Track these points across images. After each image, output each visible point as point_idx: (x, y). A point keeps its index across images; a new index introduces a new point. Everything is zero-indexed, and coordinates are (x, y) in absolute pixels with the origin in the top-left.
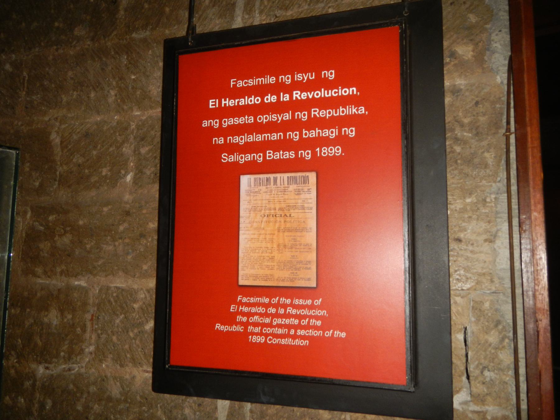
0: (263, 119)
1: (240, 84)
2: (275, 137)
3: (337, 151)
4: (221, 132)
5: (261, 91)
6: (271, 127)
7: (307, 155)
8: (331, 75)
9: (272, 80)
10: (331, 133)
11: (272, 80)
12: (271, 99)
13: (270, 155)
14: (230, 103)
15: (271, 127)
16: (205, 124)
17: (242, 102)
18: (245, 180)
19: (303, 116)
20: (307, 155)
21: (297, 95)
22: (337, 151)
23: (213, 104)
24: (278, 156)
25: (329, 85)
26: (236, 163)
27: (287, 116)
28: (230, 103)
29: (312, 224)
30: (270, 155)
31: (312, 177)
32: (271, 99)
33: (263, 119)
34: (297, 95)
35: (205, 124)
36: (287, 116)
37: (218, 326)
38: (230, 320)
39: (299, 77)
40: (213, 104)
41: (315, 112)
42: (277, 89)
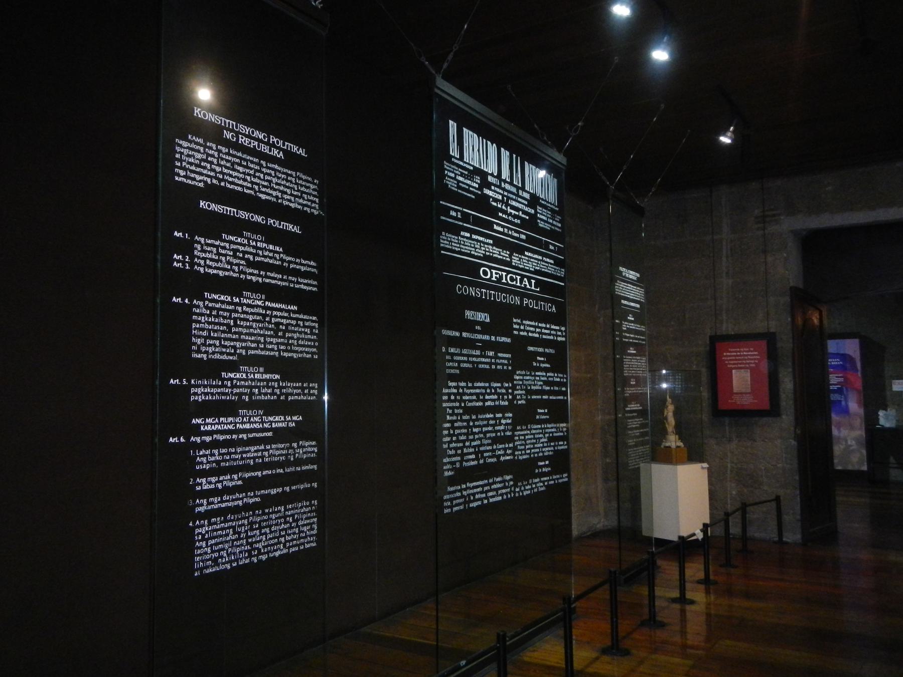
0: (737, 358)
1: (731, 350)
2: (740, 362)
3: (754, 365)
4: (727, 360)
5: (736, 352)
6: (739, 360)
7: (747, 366)
8: (752, 349)
9: (738, 350)
10: (753, 362)
11: (738, 350)
12: (739, 354)
13: (739, 366)
14: (728, 354)
15: (739, 360)
16: (723, 358)
17: (732, 354)
18: (734, 371)
19: (746, 358)
20: (747, 366)
21: (745, 353)
22: (754, 365)
23: (725, 354)
24: (741, 366)
25: (752, 351)
26: (731, 367)
27: (743, 357)
28: (728, 354)
29: (749, 380)
30: (739, 366)
31: (749, 370)
32: (739, 354)
33: (737, 358)
34: (745, 353)
35: (723, 358)
36: (743, 357)
37: (729, 401)
38: (732, 400)
39: (745, 349)
40: (725, 354)
41: (749, 357)
42: (740, 352)
